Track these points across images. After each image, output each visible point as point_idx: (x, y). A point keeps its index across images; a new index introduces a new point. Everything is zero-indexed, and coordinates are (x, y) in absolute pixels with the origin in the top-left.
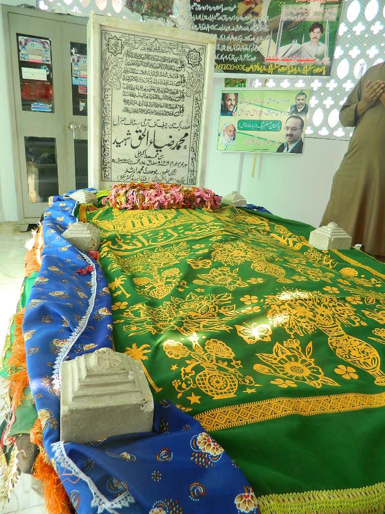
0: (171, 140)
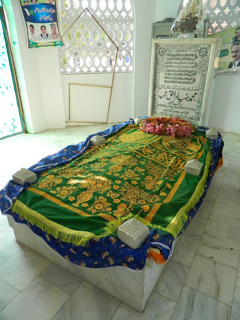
0: (187, 96)
